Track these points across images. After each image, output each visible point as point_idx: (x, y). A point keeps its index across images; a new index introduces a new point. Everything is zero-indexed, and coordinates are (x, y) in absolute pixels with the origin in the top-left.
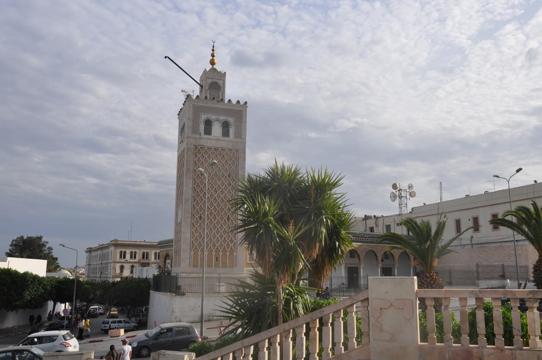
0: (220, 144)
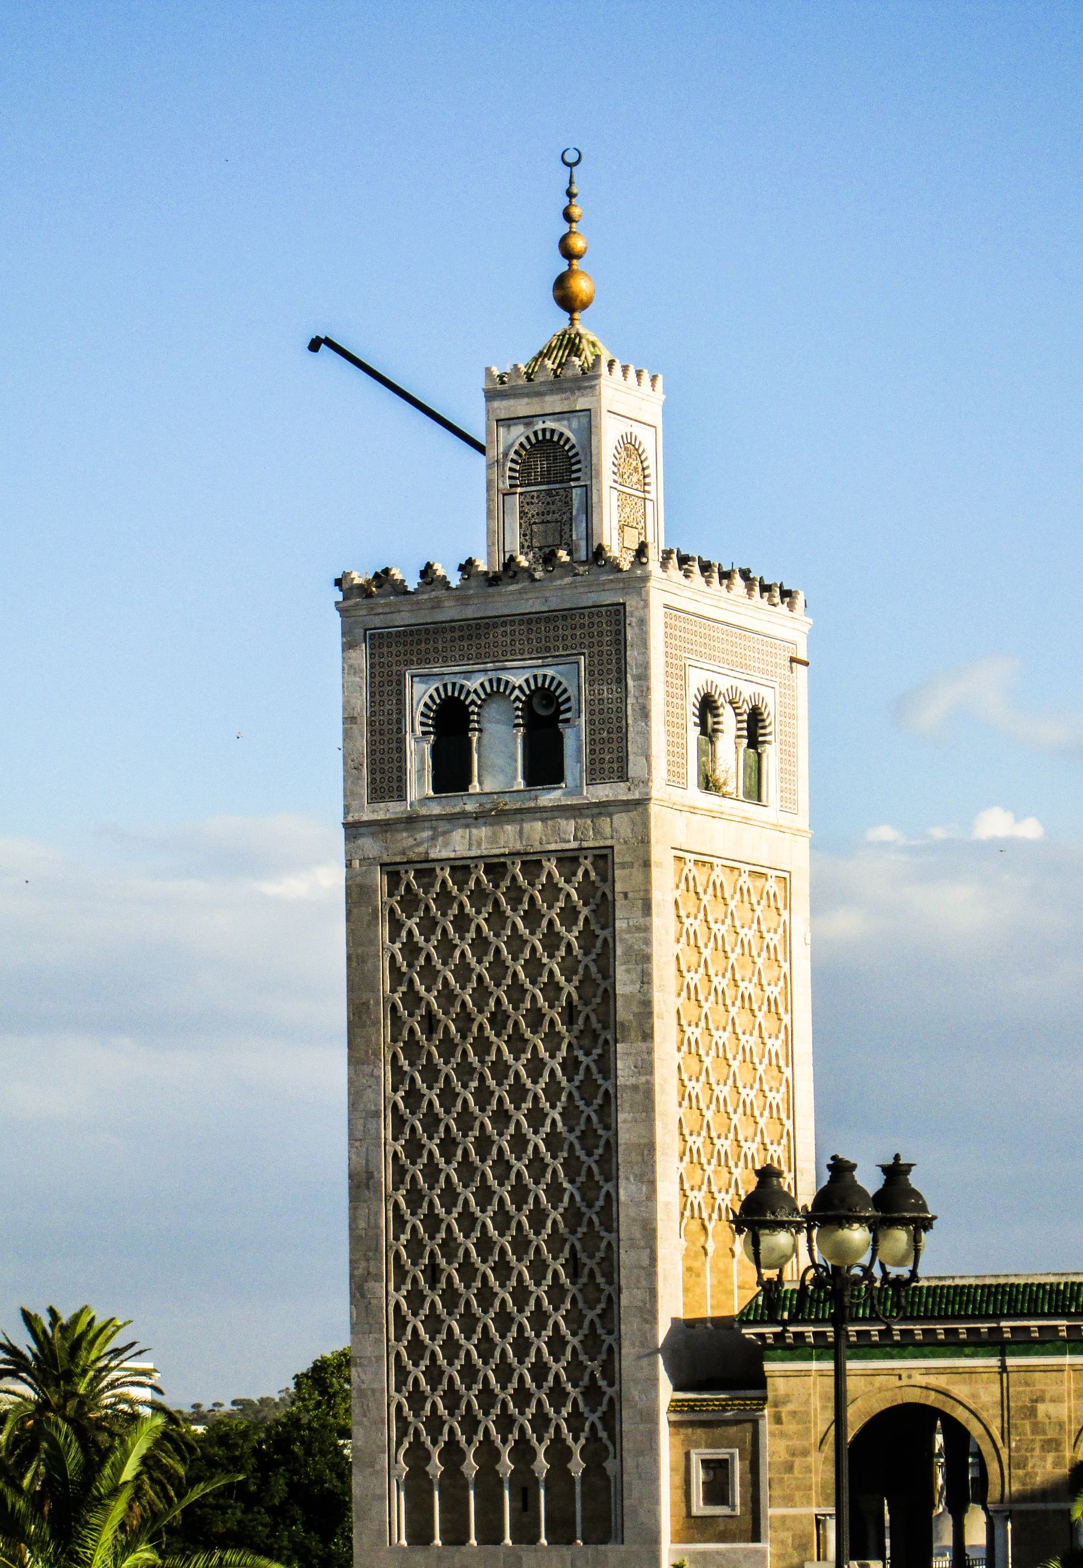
0: (508, 838)
